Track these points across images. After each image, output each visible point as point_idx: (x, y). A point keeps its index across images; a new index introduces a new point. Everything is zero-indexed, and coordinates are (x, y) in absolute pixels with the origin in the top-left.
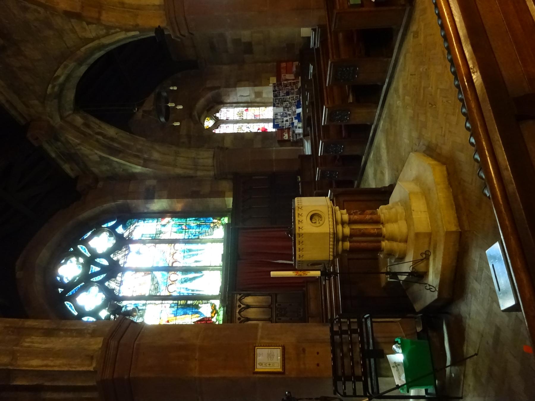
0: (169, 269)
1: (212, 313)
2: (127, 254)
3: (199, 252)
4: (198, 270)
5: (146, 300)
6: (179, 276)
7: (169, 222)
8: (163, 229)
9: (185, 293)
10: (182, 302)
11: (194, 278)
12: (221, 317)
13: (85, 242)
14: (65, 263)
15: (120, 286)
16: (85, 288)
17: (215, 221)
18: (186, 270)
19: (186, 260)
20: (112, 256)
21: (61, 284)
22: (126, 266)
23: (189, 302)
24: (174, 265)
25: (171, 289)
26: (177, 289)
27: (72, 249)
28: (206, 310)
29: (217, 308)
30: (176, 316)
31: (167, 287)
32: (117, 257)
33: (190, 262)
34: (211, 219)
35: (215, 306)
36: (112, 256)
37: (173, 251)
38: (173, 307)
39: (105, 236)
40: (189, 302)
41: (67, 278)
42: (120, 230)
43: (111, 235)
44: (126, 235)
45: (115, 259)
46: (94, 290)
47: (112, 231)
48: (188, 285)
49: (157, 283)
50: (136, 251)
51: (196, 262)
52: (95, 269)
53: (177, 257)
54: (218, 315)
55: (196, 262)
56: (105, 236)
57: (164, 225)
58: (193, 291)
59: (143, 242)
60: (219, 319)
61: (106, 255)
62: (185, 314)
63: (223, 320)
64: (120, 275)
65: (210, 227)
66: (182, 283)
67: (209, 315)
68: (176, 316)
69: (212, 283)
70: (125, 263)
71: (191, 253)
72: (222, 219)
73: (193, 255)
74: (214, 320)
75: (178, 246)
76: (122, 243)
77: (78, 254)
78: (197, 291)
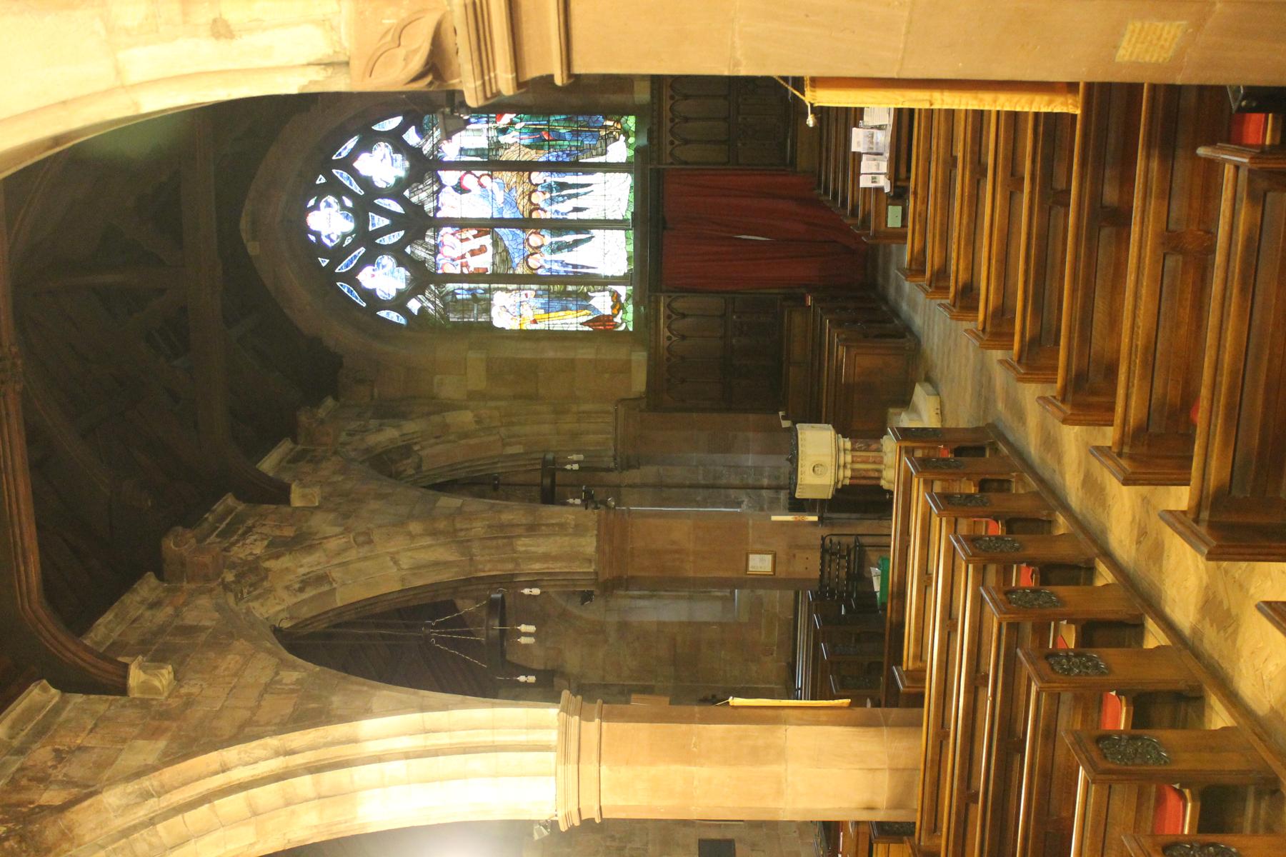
0: (526, 224)
1: (613, 307)
2: (438, 192)
3: (581, 191)
4: (584, 227)
5: (490, 283)
6: (548, 239)
7: (512, 123)
8: (503, 139)
9: (562, 271)
10: (557, 288)
11: (576, 243)
12: (630, 316)
13: (347, 164)
14: (316, 207)
15: (435, 255)
16: (368, 260)
17: (609, 123)
18: (559, 226)
19: (555, 207)
20: (407, 193)
21: (320, 249)
22: (439, 215)
23: (570, 288)
24: (535, 215)
25: (533, 262)
26: (545, 262)
27: (321, 180)
28: (602, 302)
29: (623, 299)
30: (547, 312)
31: (526, 259)
32: (420, 196)
33: (564, 209)
34: (601, 118)
35: (619, 296)
36: (407, 193)
37: (527, 187)
38: (541, 296)
39: (383, 149)
40: (570, 288)
41: (328, 237)
42: (411, 137)
43: (396, 150)
44: (427, 149)
45: (414, 200)
46: (387, 261)
47: (395, 139)
48: (565, 256)
49: (506, 250)
50: (455, 182)
51: (576, 210)
52: (379, 222)
53: (538, 198)
54: (625, 312)
55: (576, 210)
56: (383, 149)
57: (504, 131)
58: (575, 266)
59: (467, 167)
60: (626, 320)
61: (396, 192)
62: (565, 309)
63: (634, 320)
64: (429, 233)
65: (599, 138)
66: (553, 251)
67: (608, 312)
68: (547, 312)
69: (610, 254)
70: (437, 209)
71: (565, 192)
72: (623, 120)
73: (570, 197)
74: (618, 320)
75: (537, 177)
76: (424, 167)
77: (337, 189)
78: (583, 267)
